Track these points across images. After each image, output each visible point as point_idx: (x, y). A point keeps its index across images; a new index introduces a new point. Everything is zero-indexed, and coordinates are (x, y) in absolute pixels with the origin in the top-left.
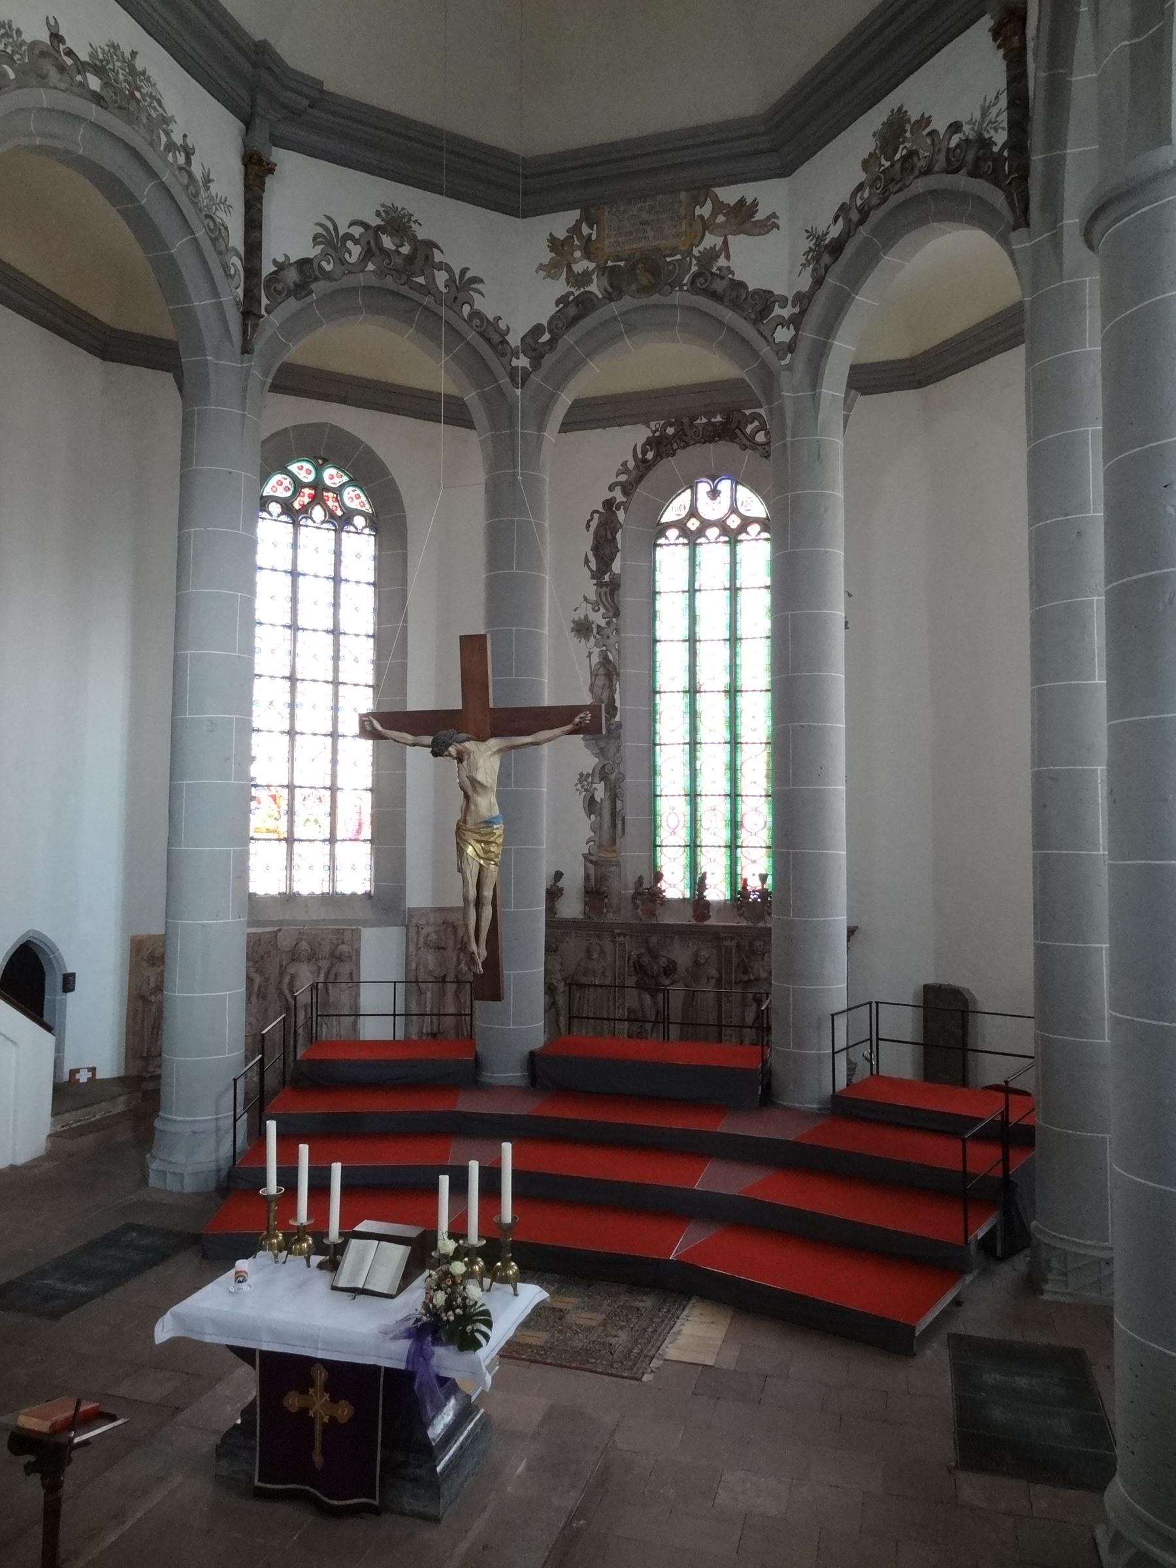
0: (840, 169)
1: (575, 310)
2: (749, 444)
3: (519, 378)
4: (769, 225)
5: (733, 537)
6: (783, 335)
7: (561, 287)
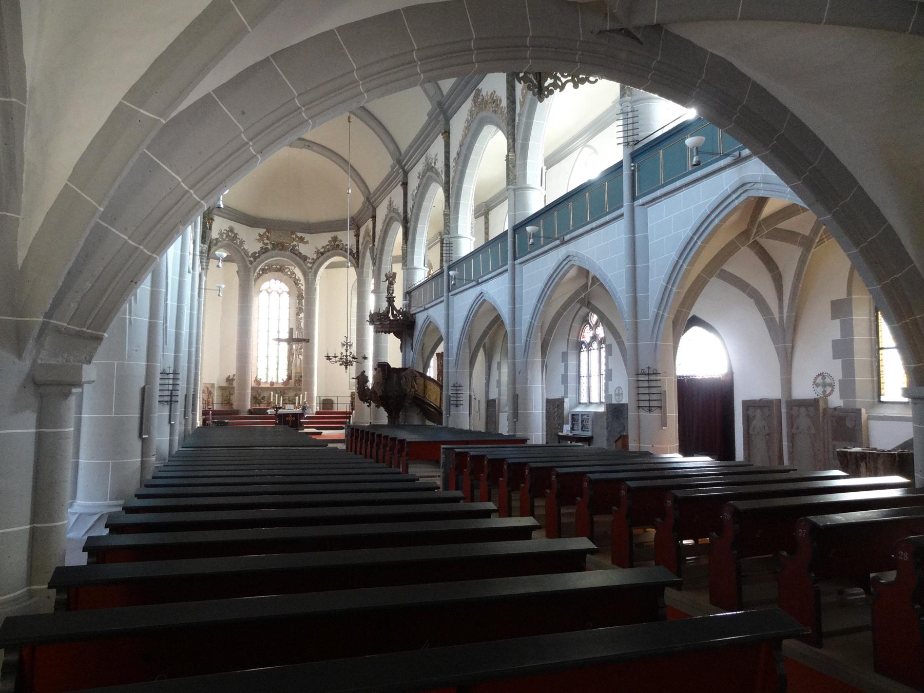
0: (323, 240)
1: (264, 251)
2: (286, 274)
3: (251, 263)
4: (307, 243)
5: (279, 294)
6: (310, 265)
7: (261, 245)
